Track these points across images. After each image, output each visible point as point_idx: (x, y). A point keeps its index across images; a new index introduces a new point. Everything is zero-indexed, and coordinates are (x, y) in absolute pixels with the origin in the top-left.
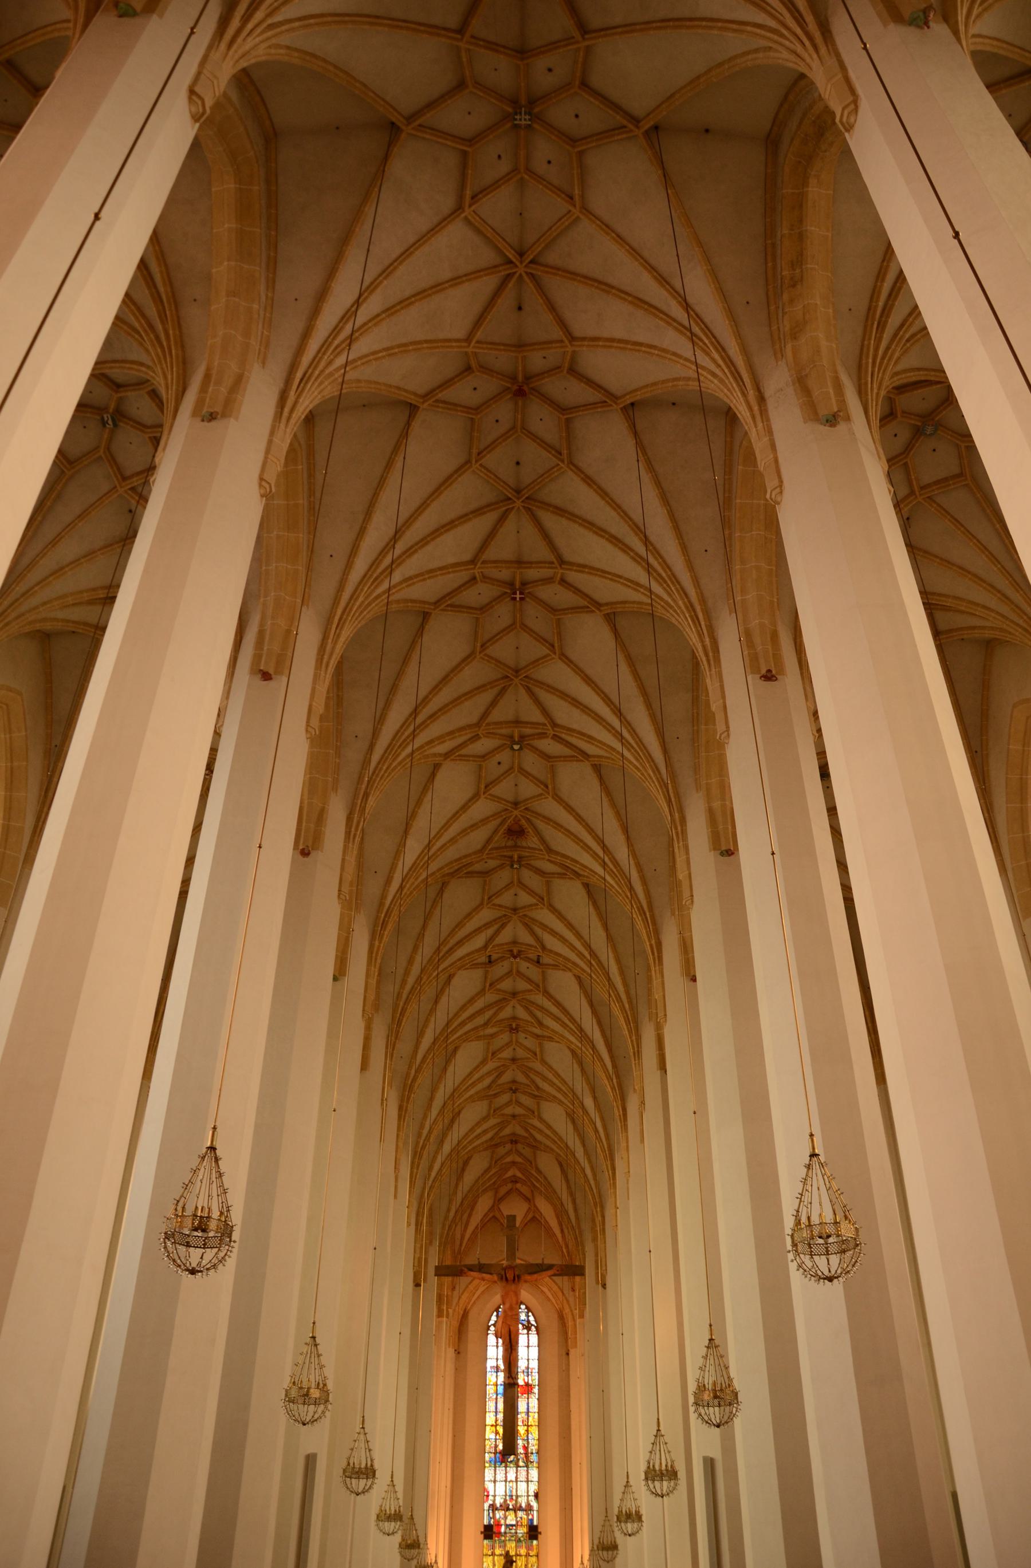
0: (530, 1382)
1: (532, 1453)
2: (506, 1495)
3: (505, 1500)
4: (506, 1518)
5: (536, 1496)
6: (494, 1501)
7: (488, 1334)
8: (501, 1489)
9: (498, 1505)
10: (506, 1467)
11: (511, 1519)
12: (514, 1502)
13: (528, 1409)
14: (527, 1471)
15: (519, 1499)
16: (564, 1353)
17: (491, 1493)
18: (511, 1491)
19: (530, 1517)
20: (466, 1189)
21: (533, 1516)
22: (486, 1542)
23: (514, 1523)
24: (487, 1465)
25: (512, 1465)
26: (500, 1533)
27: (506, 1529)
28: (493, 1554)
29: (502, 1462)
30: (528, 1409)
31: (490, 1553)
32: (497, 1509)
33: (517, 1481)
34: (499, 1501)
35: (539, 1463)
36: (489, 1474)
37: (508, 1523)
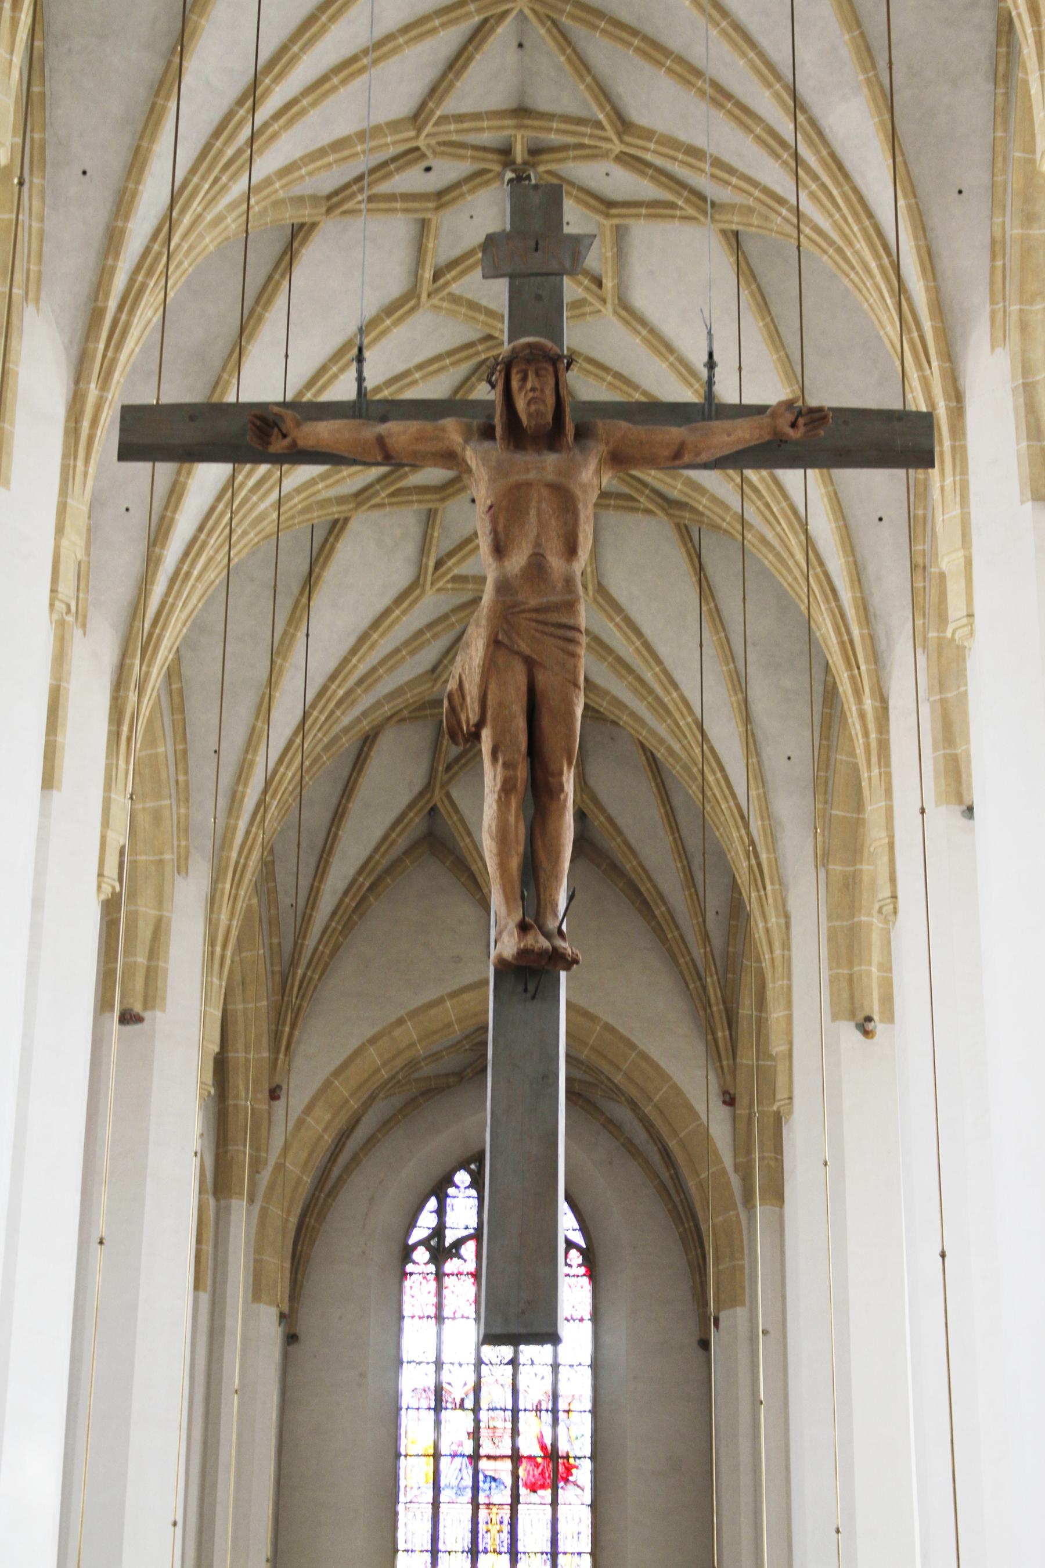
0: (563, 1448)
7: (404, 1275)
13: (554, 1541)
16: (694, 1342)
20: (322, 664)
30: (554, 1541)
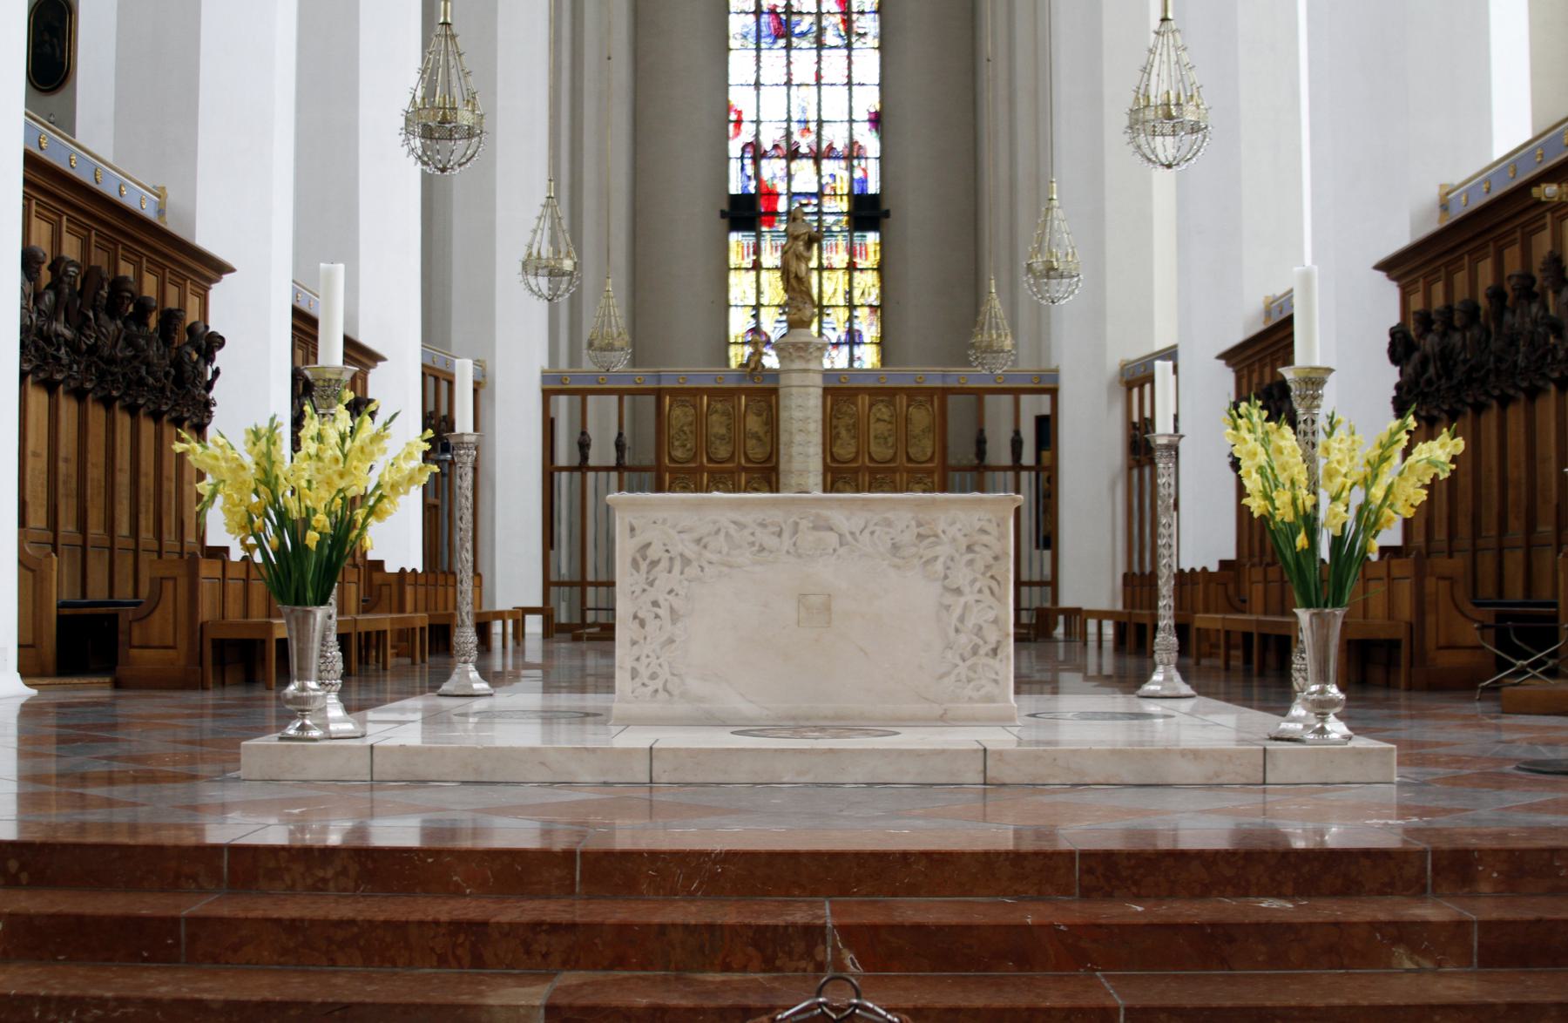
1: (862, 13)
2: (789, 120)
3: (789, 134)
4: (789, 176)
5: (876, 120)
6: (757, 135)
8: (773, 105)
9: (767, 145)
10: (788, 47)
11: (805, 177)
12: (812, 138)
14: (849, 57)
15: (827, 131)
17: (749, 115)
18: (804, 110)
19: (858, 174)
21: (865, 170)
22: (734, 237)
23: (815, 189)
24: (733, 43)
25: (804, 44)
26: (774, 213)
27: (790, 204)
28: (757, 266)
29: (777, 37)
31: (748, 263)
32: (764, 155)
33: (819, 84)
34: (770, 136)
35: (882, 37)
36: (740, 64)
37: (794, 189)
